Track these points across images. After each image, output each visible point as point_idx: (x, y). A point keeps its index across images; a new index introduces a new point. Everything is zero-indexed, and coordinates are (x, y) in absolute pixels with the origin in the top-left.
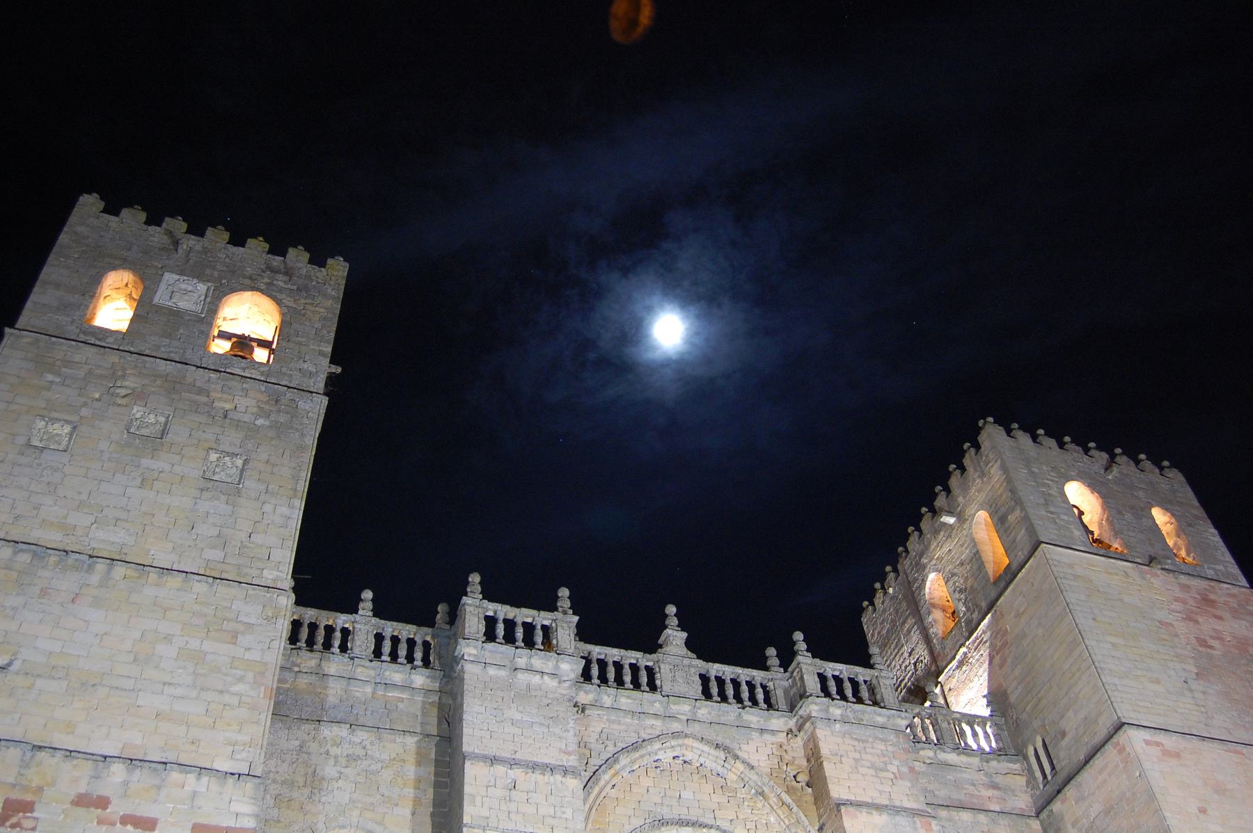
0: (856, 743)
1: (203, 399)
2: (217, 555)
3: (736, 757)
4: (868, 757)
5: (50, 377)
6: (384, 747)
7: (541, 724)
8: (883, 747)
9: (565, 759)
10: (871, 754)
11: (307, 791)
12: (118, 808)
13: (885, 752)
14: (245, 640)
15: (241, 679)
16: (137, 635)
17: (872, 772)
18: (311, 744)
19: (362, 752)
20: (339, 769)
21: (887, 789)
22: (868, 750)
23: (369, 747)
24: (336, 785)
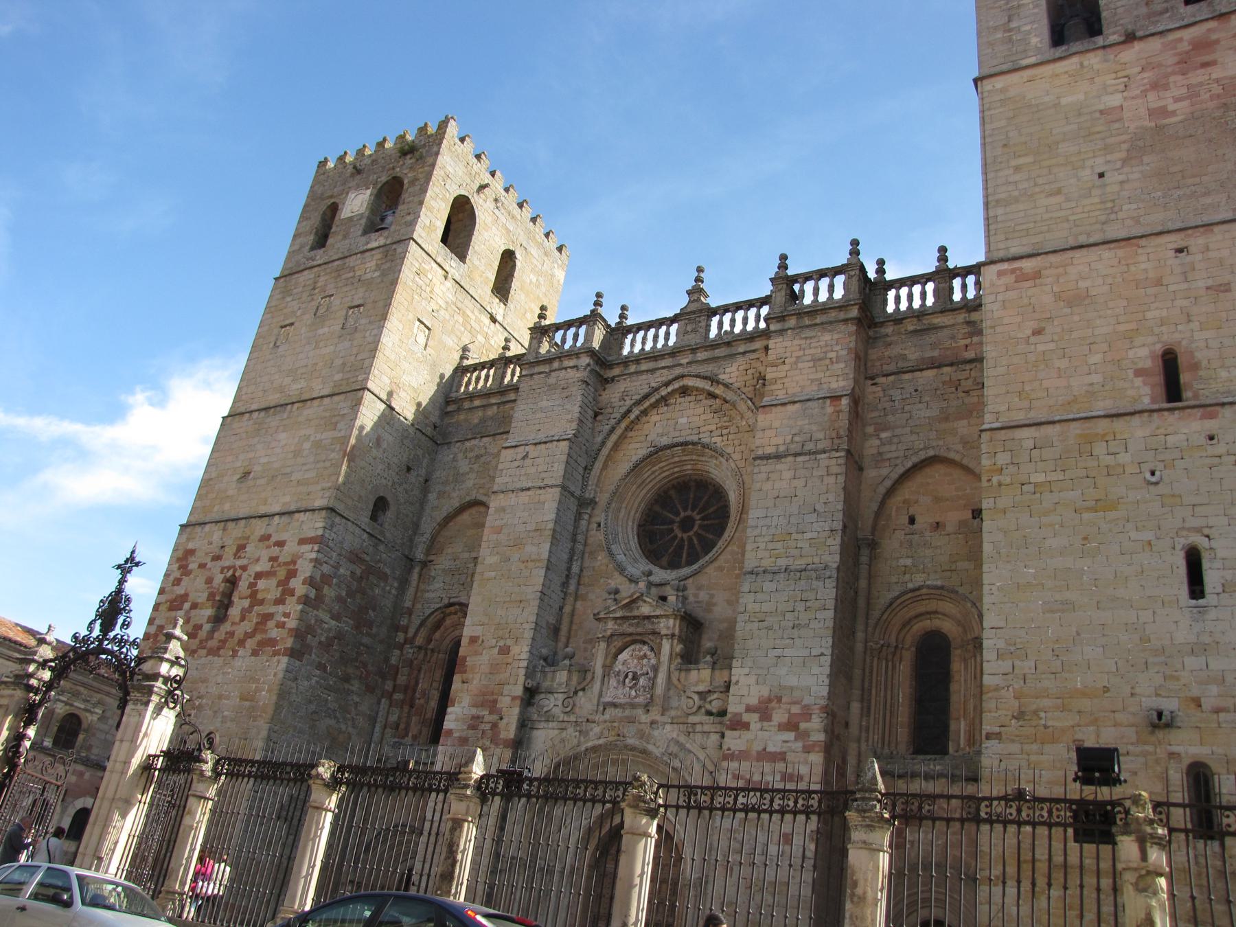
0: (803, 341)
1: (351, 274)
2: (338, 377)
3: (718, 382)
4: (812, 351)
5: (289, 299)
7: (559, 405)
8: (830, 338)
10: (816, 348)
11: (452, 486)
12: (273, 539)
14: (339, 426)
15: (333, 451)
16: (296, 440)
17: (811, 364)
21: (820, 375)
22: (812, 345)
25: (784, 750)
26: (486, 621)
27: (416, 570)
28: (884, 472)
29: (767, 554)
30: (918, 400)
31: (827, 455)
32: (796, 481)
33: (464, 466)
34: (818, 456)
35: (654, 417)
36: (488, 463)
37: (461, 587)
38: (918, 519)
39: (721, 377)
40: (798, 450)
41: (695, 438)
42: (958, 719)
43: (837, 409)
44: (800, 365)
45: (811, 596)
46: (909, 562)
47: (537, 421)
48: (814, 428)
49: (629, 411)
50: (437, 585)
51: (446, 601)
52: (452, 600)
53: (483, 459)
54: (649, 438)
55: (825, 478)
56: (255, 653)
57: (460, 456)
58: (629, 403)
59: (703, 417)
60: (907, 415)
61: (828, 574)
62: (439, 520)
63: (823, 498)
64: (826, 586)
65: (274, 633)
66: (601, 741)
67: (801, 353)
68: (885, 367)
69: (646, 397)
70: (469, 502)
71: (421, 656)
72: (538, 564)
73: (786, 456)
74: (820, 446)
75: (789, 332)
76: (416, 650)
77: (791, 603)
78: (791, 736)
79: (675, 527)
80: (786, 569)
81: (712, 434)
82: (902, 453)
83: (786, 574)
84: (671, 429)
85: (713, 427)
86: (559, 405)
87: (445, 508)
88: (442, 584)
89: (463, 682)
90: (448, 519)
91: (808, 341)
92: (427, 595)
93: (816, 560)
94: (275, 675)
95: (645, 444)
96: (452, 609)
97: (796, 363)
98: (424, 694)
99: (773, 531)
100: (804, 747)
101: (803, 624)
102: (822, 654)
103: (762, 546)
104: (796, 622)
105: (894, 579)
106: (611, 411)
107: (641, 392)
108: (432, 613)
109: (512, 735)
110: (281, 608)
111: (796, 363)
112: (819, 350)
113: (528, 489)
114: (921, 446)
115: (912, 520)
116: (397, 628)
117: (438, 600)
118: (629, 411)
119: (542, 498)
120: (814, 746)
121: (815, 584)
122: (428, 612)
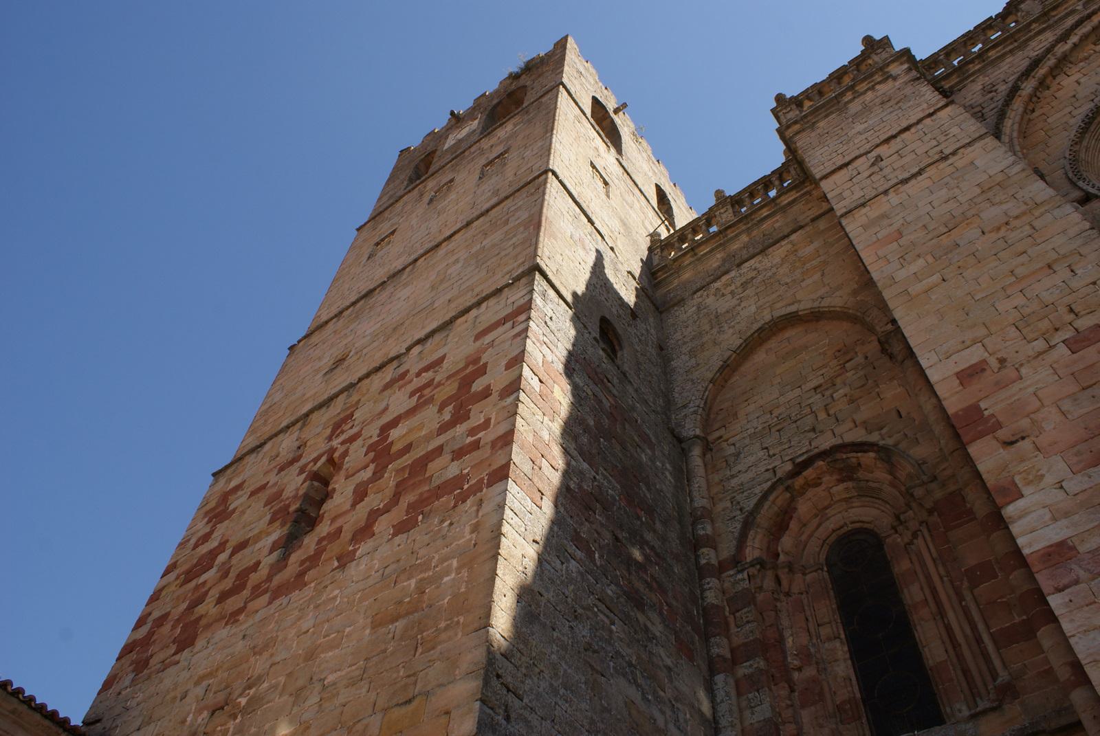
11: (715, 331)
18: (707, 301)
19: (756, 272)
20: (738, 297)
24: (739, 308)
26: (982, 332)
27: (696, 452)
37: (812, 435)
49: (1014, 91)
50: (752, 459)
51: (789, 467)
56: (402, 528)
62: (710, 375)
65: (453, 470)
70: (761, 330)
71: (769, 583)
72: (1037, 213)
76: (753, 571)
87: (715, 358)
88: (761, 454)
89: (1012, 443)
90: (728, 368)
92: (734, 482)
94: (476, 528)
96: (809, 473)
98: (806, 656)
108: (765, 497)
110: (461, 429)
113: (920, 173)
116: (696, 544)
117: (769, 475)
118: (1014, 91)
122: (750, 504)
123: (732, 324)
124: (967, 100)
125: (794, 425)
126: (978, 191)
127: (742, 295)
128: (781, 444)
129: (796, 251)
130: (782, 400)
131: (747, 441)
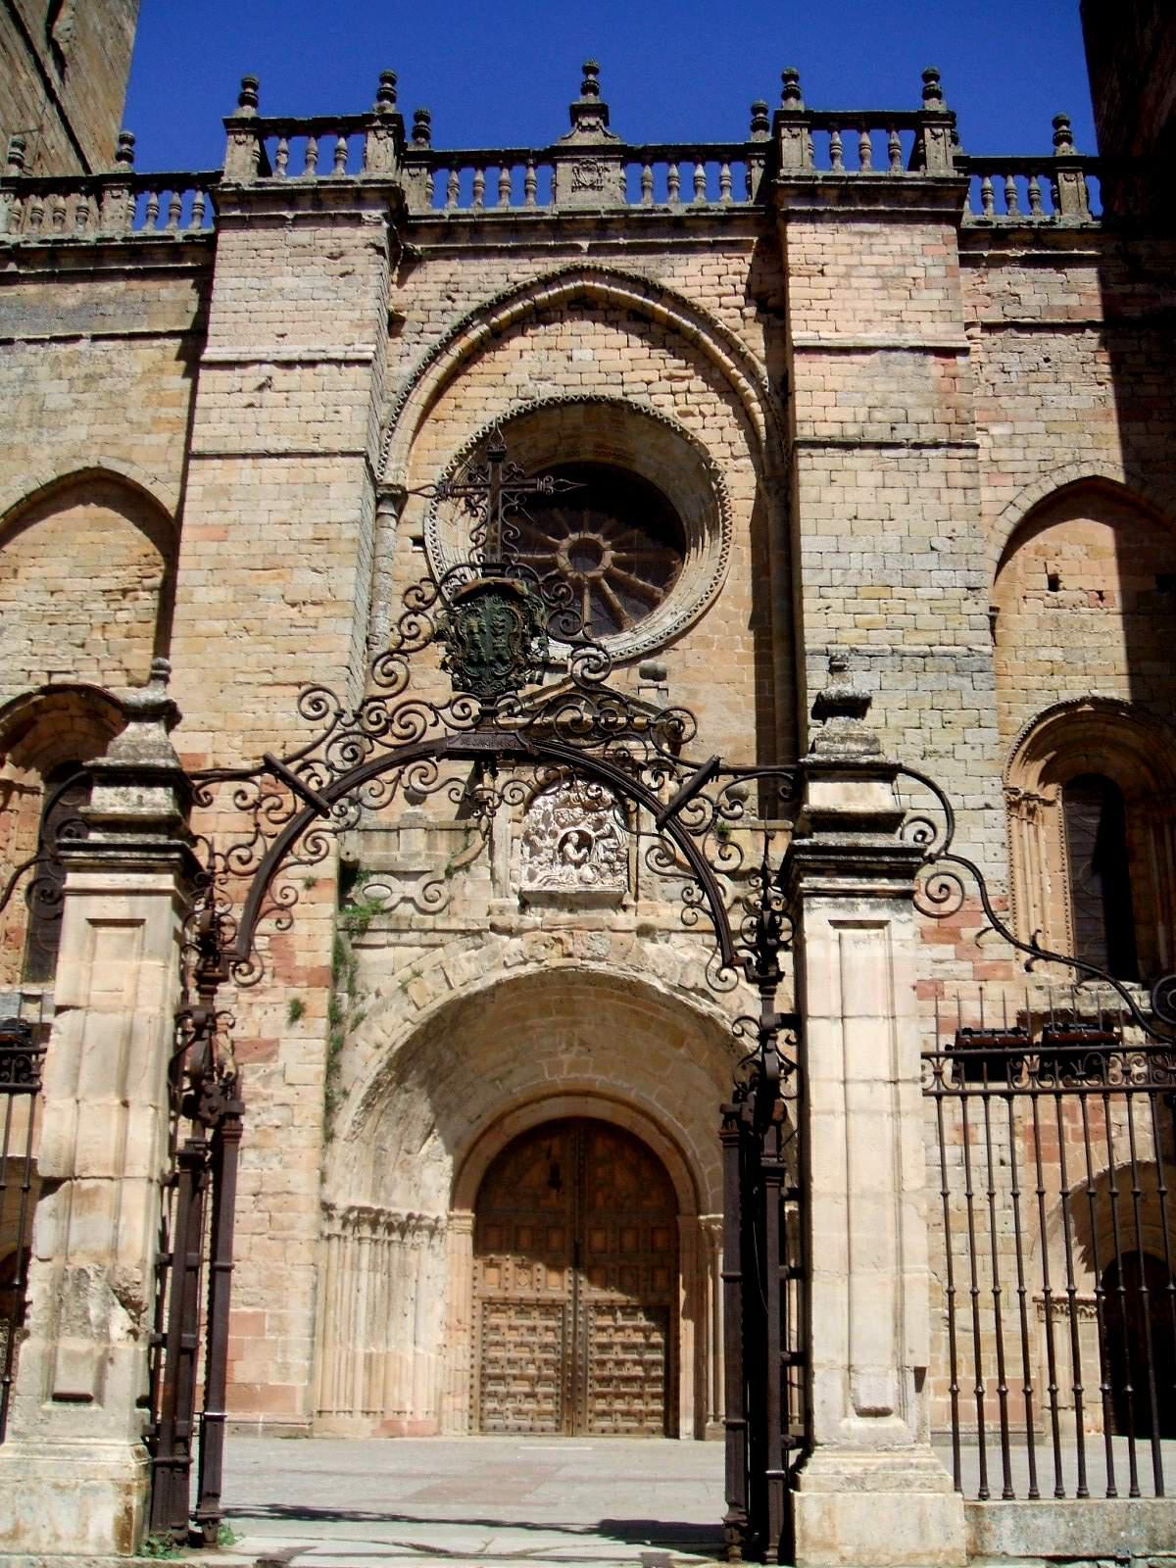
0: (857, 240)
4: (877, 259)
6: (136, 355)
7: (326, 289)
8: (907, 241)
9: (356, 336)
11: (32, 433)
13: (908, 248)
17: (877, 282)
20: (74, 396)
22: (875, 249)
23: (115, 359)
24: (70, 418)
25: (938, 976)
26: (218, 723)
28: (1008, 494)
29: (848, 621)
30: (1051, 377)
31: (942, 451)
32: (887, 491)
33: (56, 394)
34: (926, 452)
35: (517, 343)
36: (123, 393)
37: (79, 653)
38: (1065, 581)
39: (666, 282)
40: (887, 438)
41: (616, 393)
42: (1151, 924)
43: (951, 371)
44: (855, 282)
45: (952, 701)
46: (1057, 655)
47: (279, 316)
48: (910, 400)
50: (12, 646)
52: (57, 679)
53: (106, 385)
54: (514, 379)
55: (945, 493)
57: (43, 371)
58: (464, 307)
59: (626, 352)
60: (1037, 401)
61: (977, 665)
63: (945, 528)
64: (977, 684)
66: (531, 968)
67: (855, 260)
68: (981, 310)
69: (503, 301)
73: (862, 445)
74: (926, 436)
75: (827, 216)
77: (913, 713)
78: (947, 950)
79: (563, 561)
80: (893, 651)
81: (652, 388)
82: (1034, 466)
83: (897, 658)
84: (559, 369)
85: (653, 376)
86: (326, 289)
87: (18, 480)
91: (866, 240)
93: (947, 638)
95: (498, 392)
97: (847, 276)
99: (855, 581)
100: (975, 971)
101: (942, 749)
102: (988, 807)
103: (837, 604)
104: (930, 748)
105: (1034, 682)
106: (423, 318)
107: (487, 287)
109: (326, 959)
111: (847, 276)
112: (888, 260)
114: (1069, 458)
115: (1054, 583)
119: (322, 474)
120: (994, 968)
121: (955, 681)
123: (54, 439)
124: (426, 287)
125: (67, 628)
126: (310, 534)
127: (82, 397)
128: (47, 645)
129: (161, 371)
130: (67, 584)
131: (16, 617)
